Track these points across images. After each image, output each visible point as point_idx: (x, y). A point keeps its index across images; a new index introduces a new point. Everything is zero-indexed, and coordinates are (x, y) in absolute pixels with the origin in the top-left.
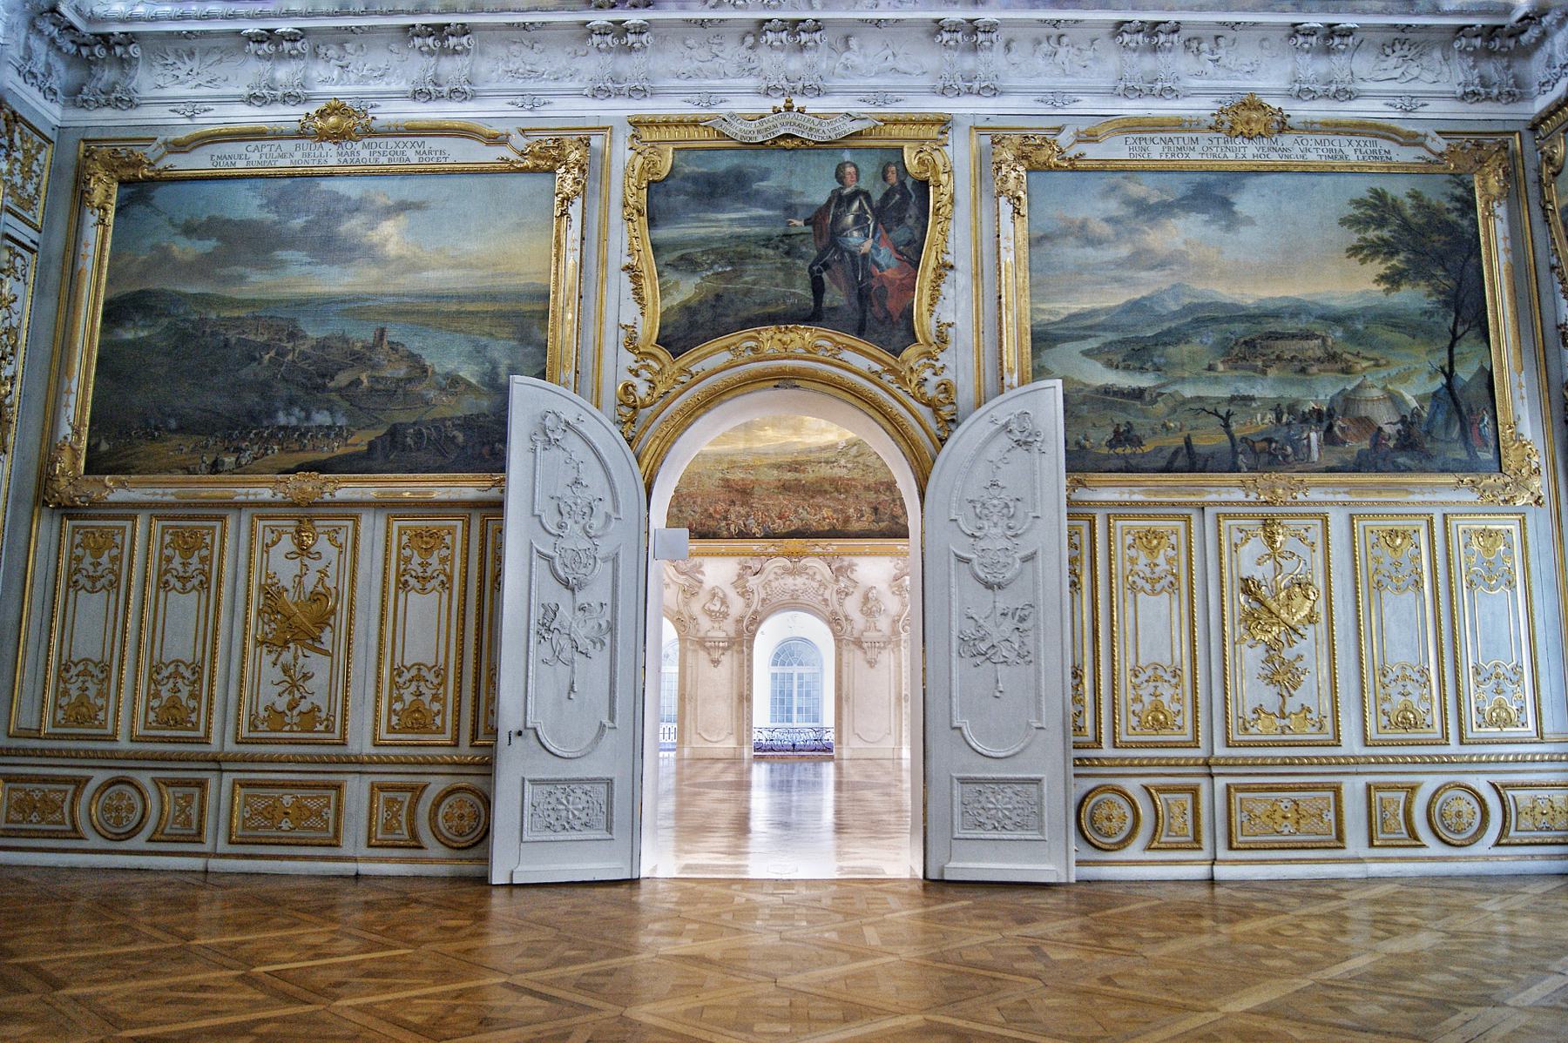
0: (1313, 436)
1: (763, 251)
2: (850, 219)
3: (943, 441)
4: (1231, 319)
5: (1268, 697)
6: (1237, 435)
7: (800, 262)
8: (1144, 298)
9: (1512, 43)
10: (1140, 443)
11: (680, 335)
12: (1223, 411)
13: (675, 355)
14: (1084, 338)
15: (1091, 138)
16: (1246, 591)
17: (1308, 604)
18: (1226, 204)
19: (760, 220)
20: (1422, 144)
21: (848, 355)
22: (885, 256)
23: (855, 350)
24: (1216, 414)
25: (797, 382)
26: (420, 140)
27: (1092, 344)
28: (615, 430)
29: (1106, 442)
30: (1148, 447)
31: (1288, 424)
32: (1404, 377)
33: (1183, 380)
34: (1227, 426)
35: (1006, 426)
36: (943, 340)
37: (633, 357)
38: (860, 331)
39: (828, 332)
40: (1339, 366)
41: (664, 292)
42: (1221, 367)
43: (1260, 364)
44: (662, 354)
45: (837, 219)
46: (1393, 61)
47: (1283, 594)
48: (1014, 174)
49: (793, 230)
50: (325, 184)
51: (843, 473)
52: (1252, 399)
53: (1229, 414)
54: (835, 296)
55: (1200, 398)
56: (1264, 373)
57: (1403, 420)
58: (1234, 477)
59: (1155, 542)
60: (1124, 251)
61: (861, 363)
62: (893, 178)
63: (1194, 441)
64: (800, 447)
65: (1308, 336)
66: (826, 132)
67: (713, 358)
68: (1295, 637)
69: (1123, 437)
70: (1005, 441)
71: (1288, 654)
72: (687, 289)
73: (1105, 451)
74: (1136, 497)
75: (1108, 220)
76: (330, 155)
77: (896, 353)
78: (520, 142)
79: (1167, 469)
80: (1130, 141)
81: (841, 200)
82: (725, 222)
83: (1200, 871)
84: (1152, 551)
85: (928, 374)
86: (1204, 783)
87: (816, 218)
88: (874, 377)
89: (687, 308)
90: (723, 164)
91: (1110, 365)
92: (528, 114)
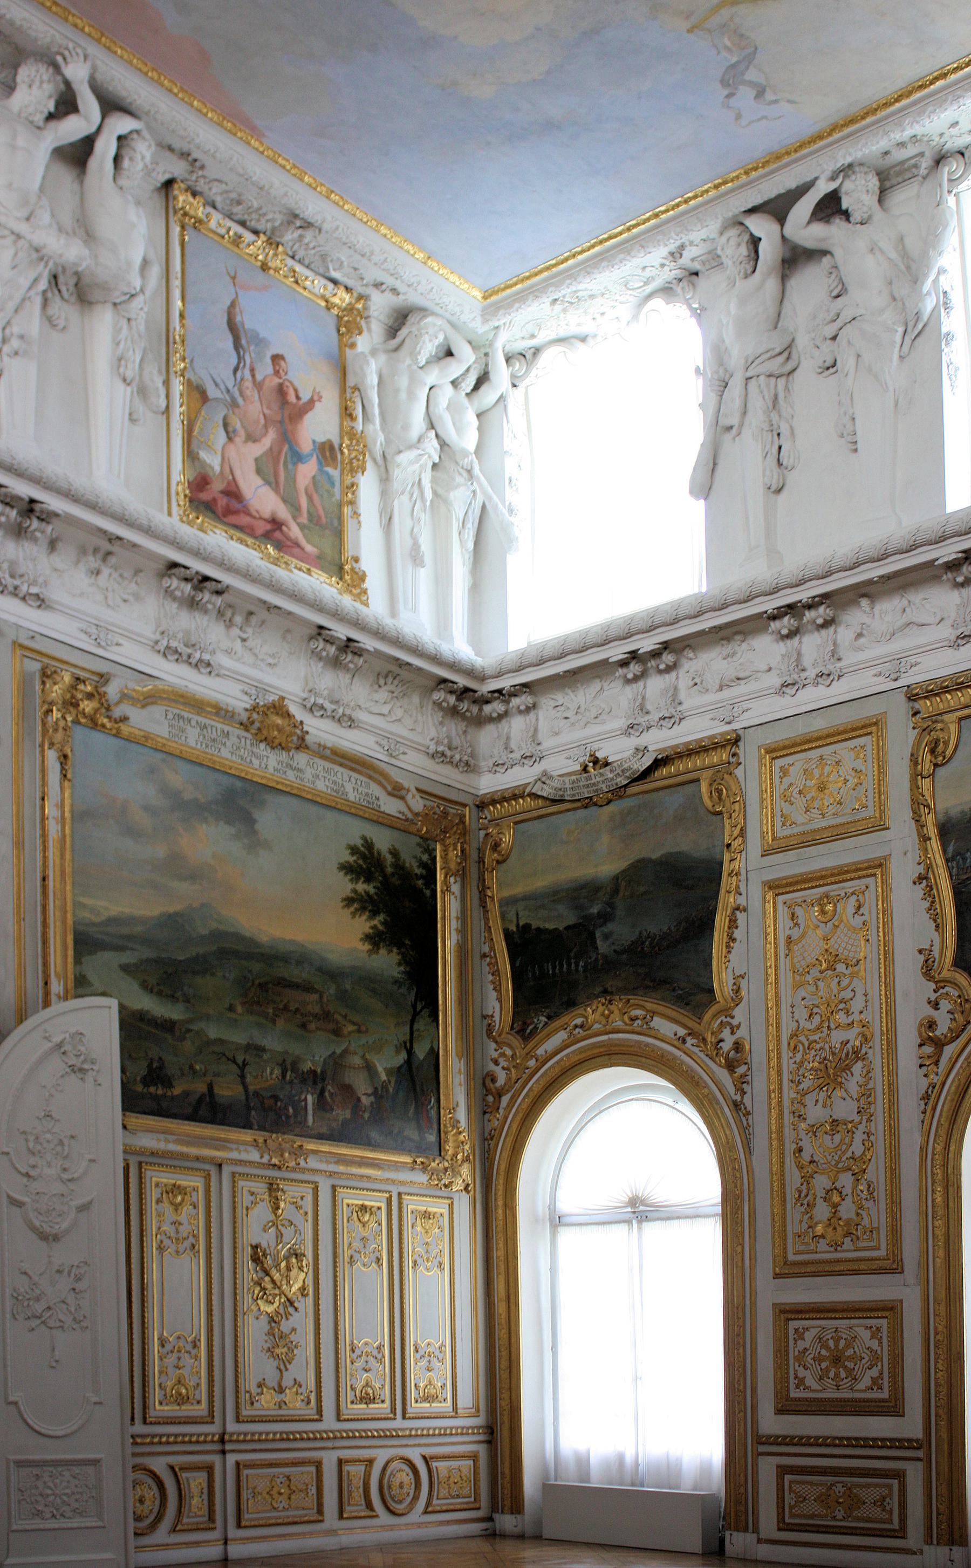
0: (310, 1098)
4: (249, 956)
5: (269, 1369)
6: (251, 1088)
9: (475, 709)
10: (170, 1086)
16: (256, 1259)
17: (302, 1275)
18: (249, 821)
20: (402, 798)
24: (234, 1061)
30: (177, 1091)
31: (291, 1082)
32: (378, 1047)
33: (208, 1017)
34: (243, 1077)
35: (60, 1045)
40: (331, 1026)
42: (239, 1009)
46: (383, 695)
47: (283, 1264)
53: (245, 1064)
55: (221, 1042)
56: (274, 1022)
57: (375, 1093)
58: (247, 1136)
63: (217, 1090)
65: (308, 988)
68: (291, 1310)
71: (285, 1326)
79: (193, 1117)
83: (215, 1552)
84: (177, 1207)
86: (216, 1459)
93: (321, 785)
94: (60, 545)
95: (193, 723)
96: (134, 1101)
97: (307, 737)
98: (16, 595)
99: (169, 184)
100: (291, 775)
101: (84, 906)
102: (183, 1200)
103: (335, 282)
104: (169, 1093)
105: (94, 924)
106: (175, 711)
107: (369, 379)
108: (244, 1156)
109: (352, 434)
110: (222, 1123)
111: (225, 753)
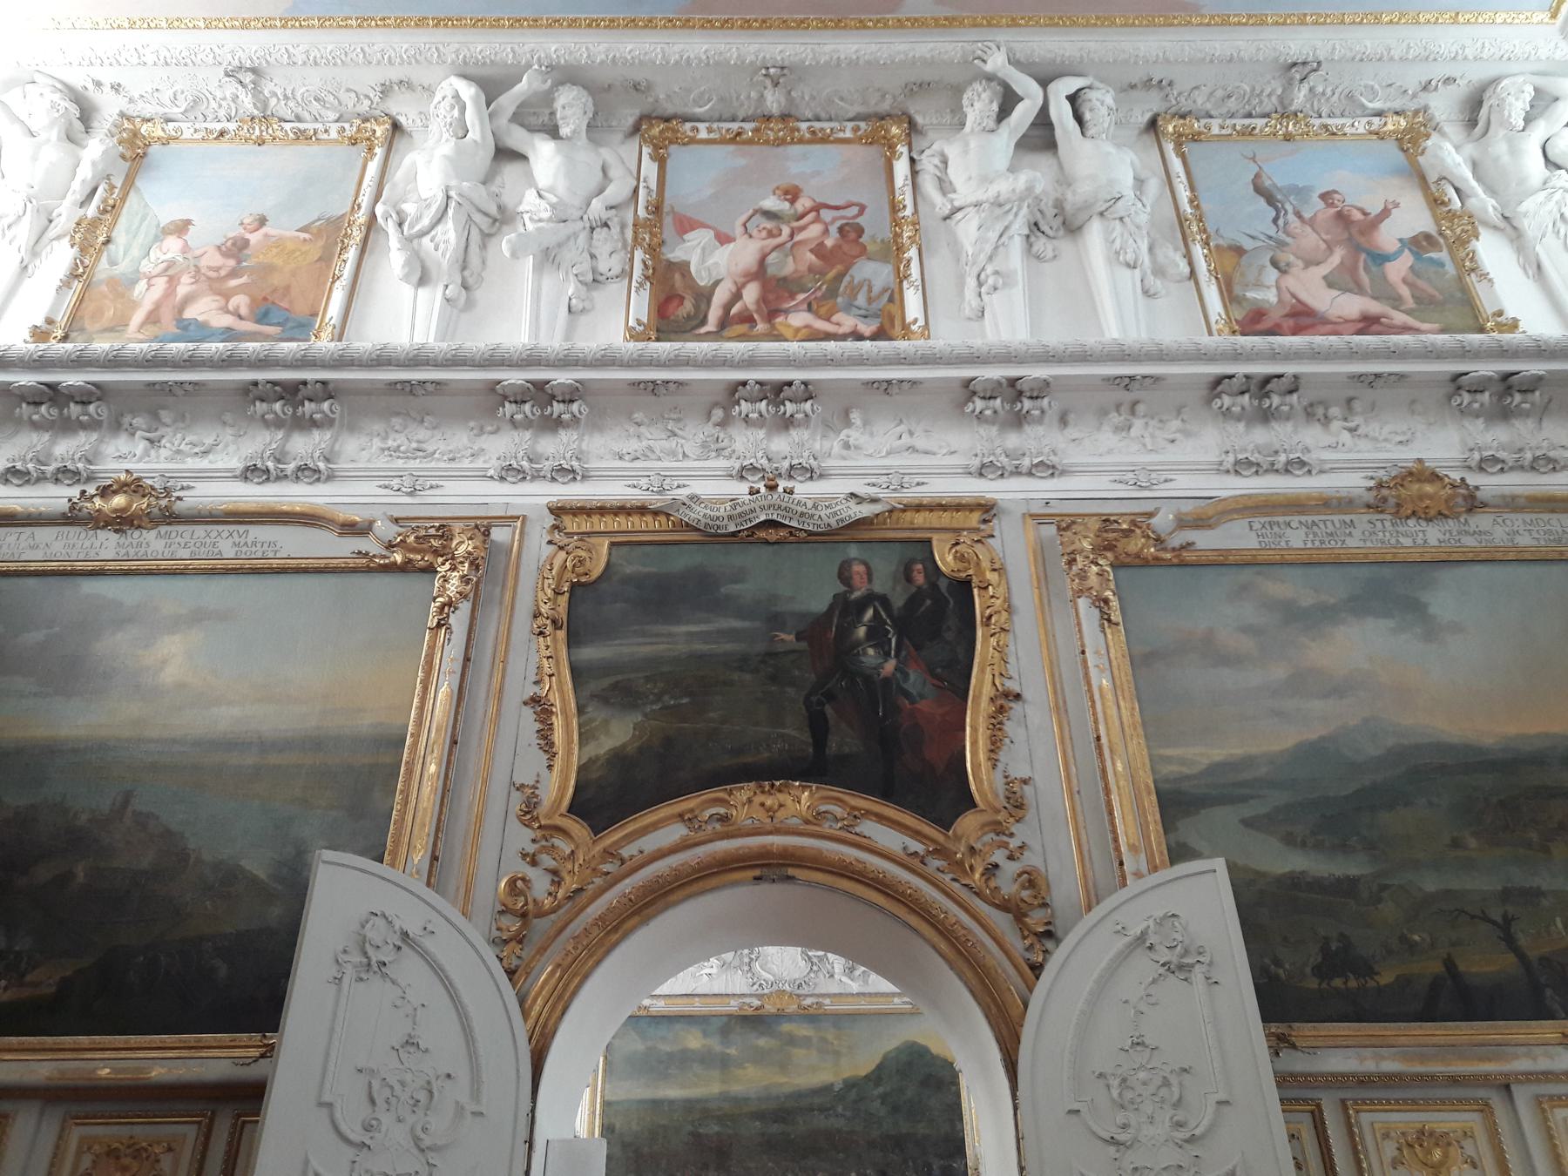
1: (736, 676)
2: (861, 632)
3: (1037, 969)
7: (791, 691)
8: (1322, 739)
10: (1371, 972)
11: (605, 799)
12: (1496, 914)
13: (597, 829)
14: (1243, 799)
15: (1200, 522)
19: (731, 634)
21: (869, 828)
22: (915, 680)
23: (881, 818)
25: (791, 871)
26: (242, 528)
27: (1247, 811)
28: (489, 954)
29: (1312, 969)
30: (1386, 978)
34: (1510, 941)
36: (1017, 805)
37: (529, 834)
38: (887, 791)
39: (836, 792)
41: (584, 738)
43: (1534, 836)
44: (579, 829)
45: (845, 632)
48: (1095, 569)
49: (780, 648)
50: (89, 586)
51: (839, 1123)
52: (1538, 893)
53: (1508, 921)
54: (844, 740)
55: (1448, 893)
59: (1437, 1154)
60: (1279, 672)
61: (891, 840)
62: (920, 579)
64: (787, 1089)
66: (825, 518)
67: (659, 836)
69: (1338, 960)
70: (1144, 966)
72: (620, 732)
73: (1313, 984)
74: (1390, 1066)
75: (1247, 629)
76: (107, 546)
77: (945, 823)
78: (385, 530)
79: (1428, 1014)
80: (1256, 526)
81: (847, 608)
82: (682, 637)
85: (999, 857)
87: (813, 630)
88: (916, 863)
89: (618, 758)
90: (680, 562)
91: (1290, 840)
92: (408, 500)
93: (1524, 540)
94: (1071, 417)
95: (1294, 525)
96: (1282, 1003)
97: (1478, 494)
98: (1020, 474)
99: (1153, 125)
100: (1469, 541)
101: (1168, 760)
102: (1446, 1155)
103: (1379, 114)
104: (1371, 984)
105: (1188, 777)
106: (1263, 520)
107: (1449, 160)
108: (1543, 1064)
109: (1452, 216)
110: (1489, 1016)
111: (1350, 542)
